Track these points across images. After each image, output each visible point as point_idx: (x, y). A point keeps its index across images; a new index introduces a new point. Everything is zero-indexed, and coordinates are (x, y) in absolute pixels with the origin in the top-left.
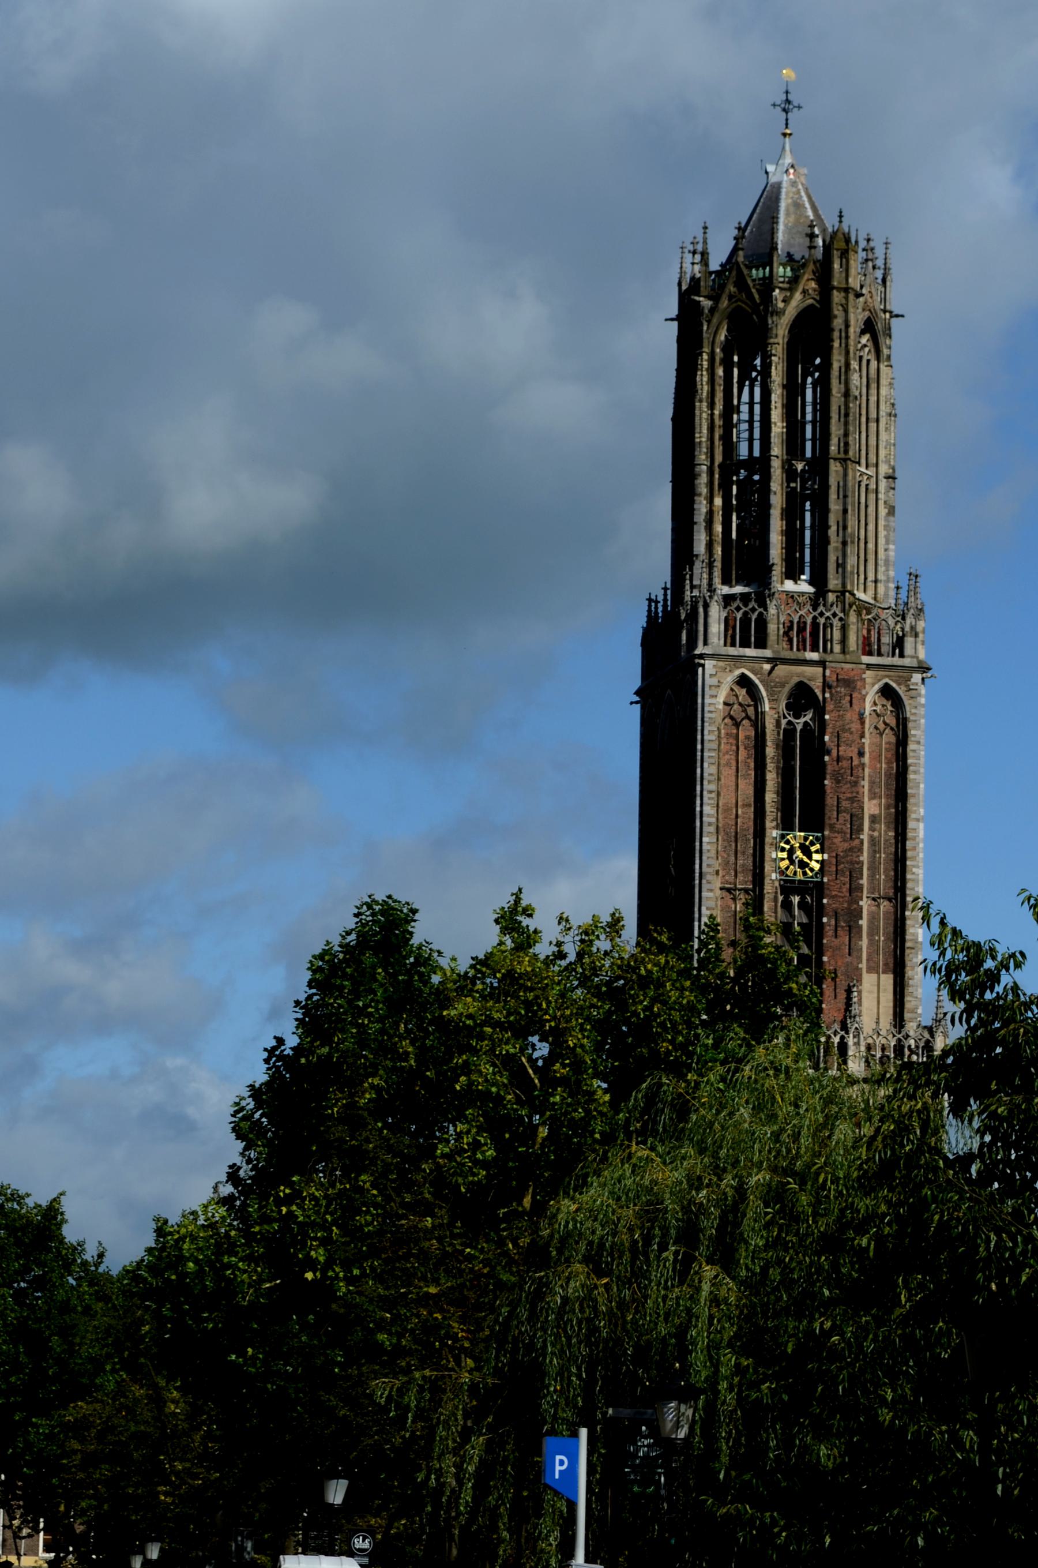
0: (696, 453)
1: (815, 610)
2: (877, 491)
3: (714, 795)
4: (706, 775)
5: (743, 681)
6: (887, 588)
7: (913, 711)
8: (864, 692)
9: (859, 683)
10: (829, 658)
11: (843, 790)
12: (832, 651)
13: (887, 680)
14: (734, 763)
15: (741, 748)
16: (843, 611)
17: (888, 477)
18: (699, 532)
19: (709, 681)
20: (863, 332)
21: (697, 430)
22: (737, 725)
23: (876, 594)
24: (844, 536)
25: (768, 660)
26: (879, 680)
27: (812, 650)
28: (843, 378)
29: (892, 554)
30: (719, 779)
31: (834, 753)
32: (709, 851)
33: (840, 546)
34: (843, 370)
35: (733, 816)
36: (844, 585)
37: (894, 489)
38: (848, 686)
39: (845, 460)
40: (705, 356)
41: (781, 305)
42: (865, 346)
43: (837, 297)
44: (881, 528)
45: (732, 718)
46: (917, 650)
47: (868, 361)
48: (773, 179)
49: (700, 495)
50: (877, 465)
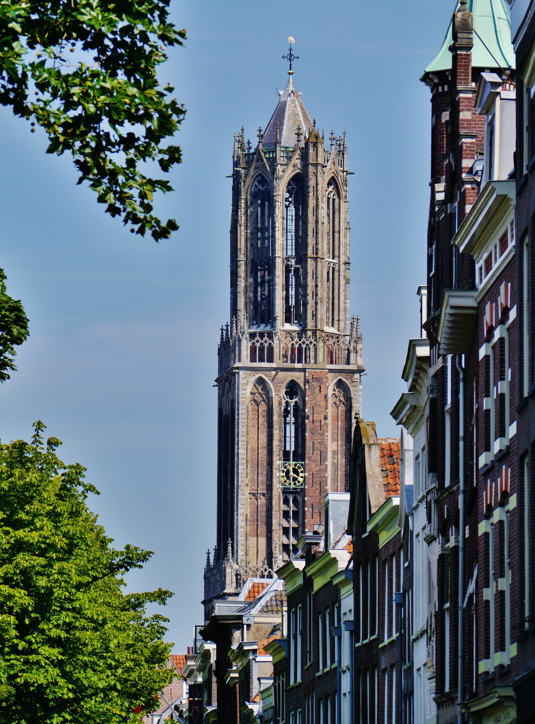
0: (239, 254)
1: (300, 340)
2: (339, 271)
3: (245, 443)
4: (240, 432)
5: (261, 381)
6: (345, 324)
7: (355, 393)
8: (327, 384)
9: (324, 379)
10: (307, 366)
11: (316, 438)
12: (310, 363)
13: (340, 377)
14: (256, 425)
15: (260, 417)
16: (316, 340)
17: (345, 263)
18: (240, 297)
19: (241, 381)
20: (329, 184)
21: (239, 241)
22: (257, 404)
23: (339, 327)
24: (316, 300)
25: (275, 369)
26: (336, 377)
27: (298, 363)
28: (315, 213)
29: (348, 305)
30: (247, 434)
31: (311, 418)
32: (242, 473)
33: (314, 304)
34: (315, 208)
35: (256, 454)
36: (316, 326)
37: (349, 269)
38: (319, 381)
39: (317, 258)
40: (243, 201)
41: (281, 173)
42: (331, 192)
43: (311, 169)
44: (341, 291)
45: (255, 401)
46: (357, 361)
47: (334, 200)
48: (283, 99)
49: (241, 277)
50: (339, 257)
